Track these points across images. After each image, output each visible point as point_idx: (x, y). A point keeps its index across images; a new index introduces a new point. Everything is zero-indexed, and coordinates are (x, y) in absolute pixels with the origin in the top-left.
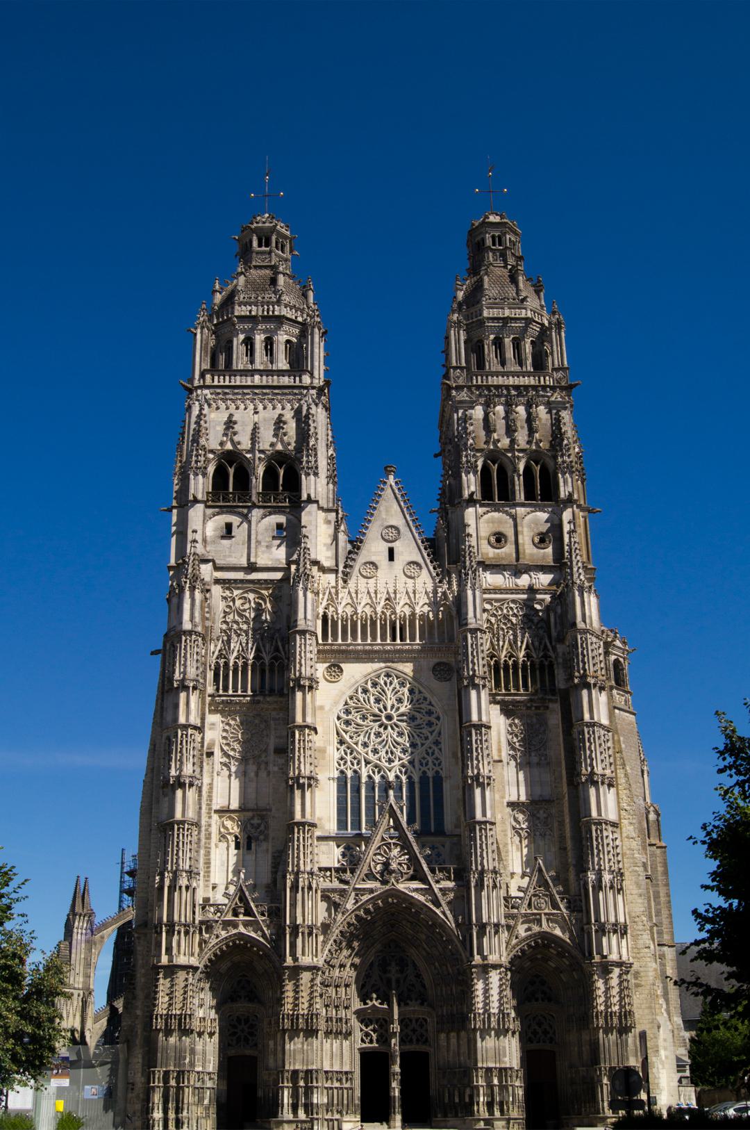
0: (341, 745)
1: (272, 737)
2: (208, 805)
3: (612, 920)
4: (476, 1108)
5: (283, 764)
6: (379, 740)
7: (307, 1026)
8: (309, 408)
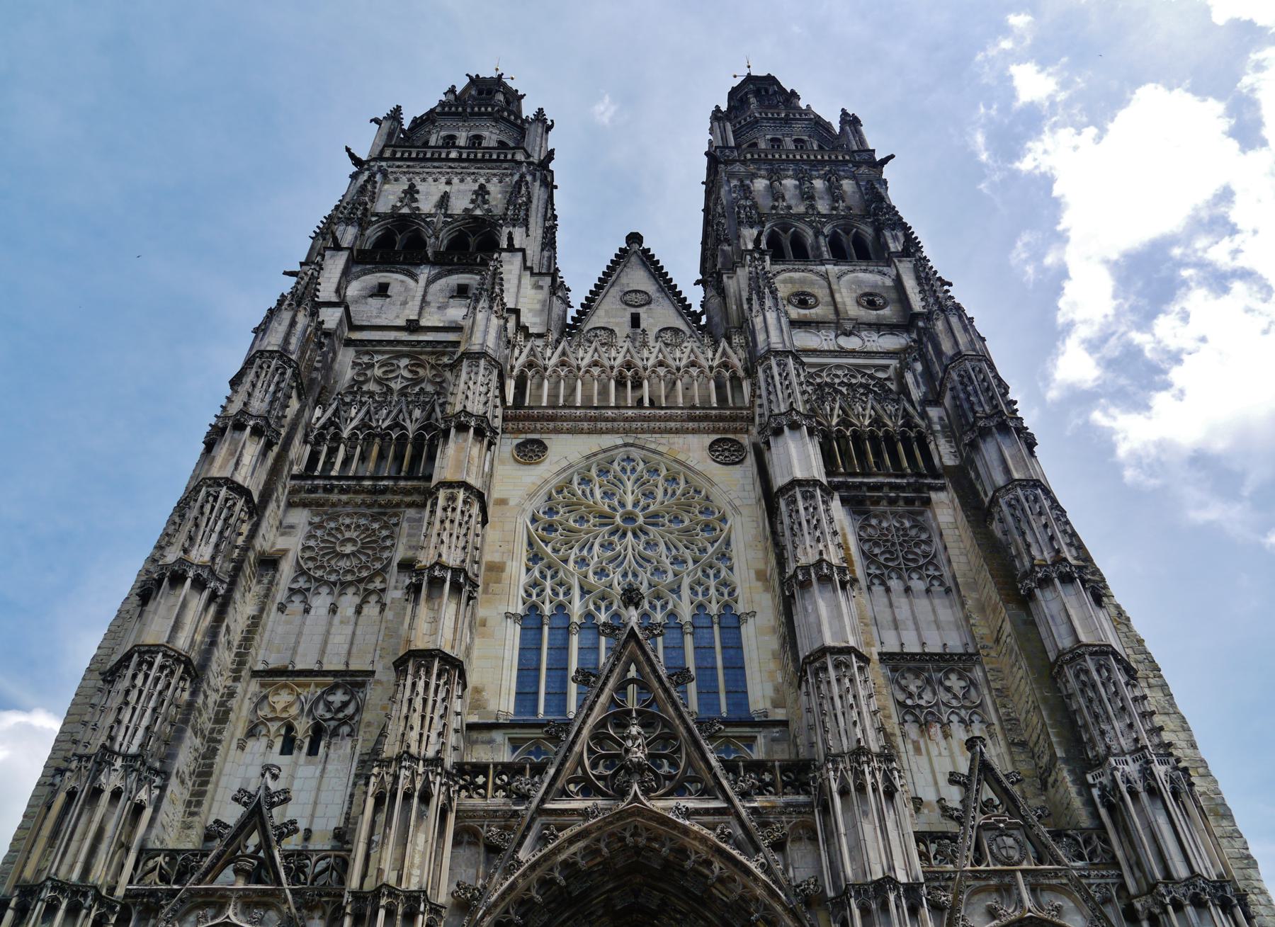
6: (609, 553)
8: (522, 176)
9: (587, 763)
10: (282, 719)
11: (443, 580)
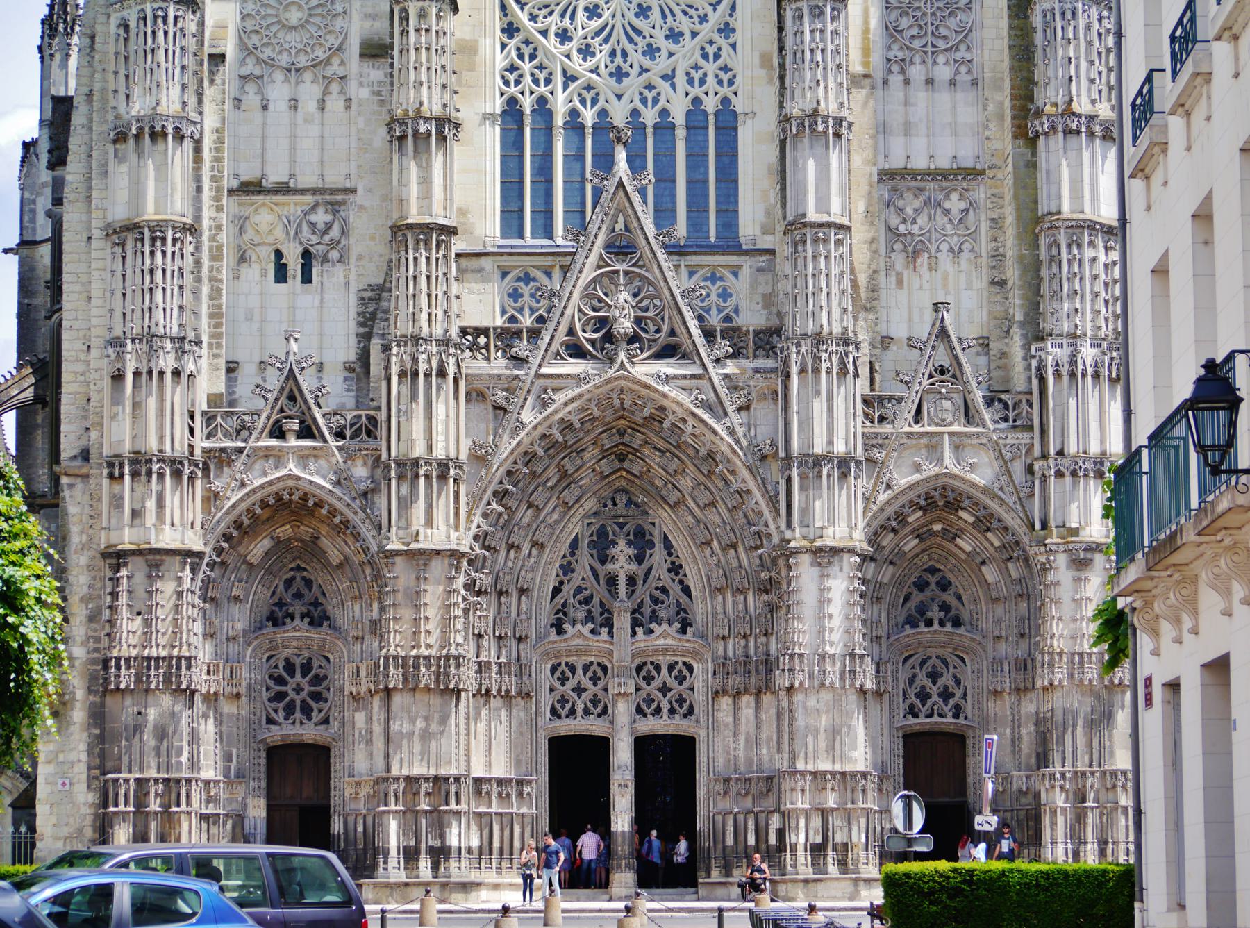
0: (511, 37)
1: (356, 17)
2: (213, 179)
3: (1094, 449)
4: (788, 857)
5: (380, 82)
6: (596, 23)
7: (437, 681)
9: (578, 325)
10: (270, 245)
11: (429, 134)
